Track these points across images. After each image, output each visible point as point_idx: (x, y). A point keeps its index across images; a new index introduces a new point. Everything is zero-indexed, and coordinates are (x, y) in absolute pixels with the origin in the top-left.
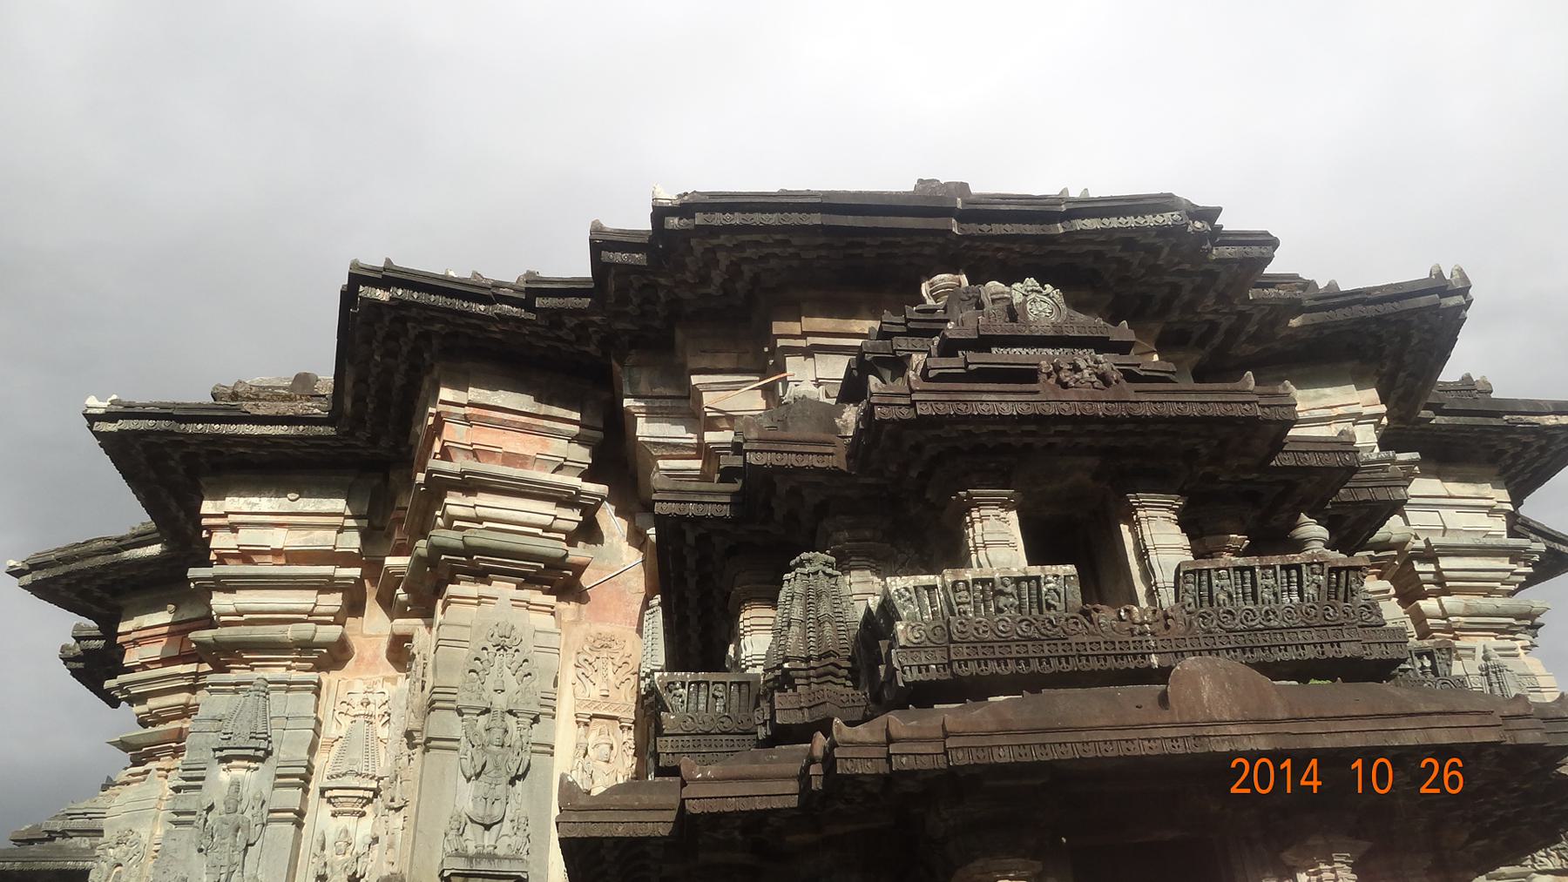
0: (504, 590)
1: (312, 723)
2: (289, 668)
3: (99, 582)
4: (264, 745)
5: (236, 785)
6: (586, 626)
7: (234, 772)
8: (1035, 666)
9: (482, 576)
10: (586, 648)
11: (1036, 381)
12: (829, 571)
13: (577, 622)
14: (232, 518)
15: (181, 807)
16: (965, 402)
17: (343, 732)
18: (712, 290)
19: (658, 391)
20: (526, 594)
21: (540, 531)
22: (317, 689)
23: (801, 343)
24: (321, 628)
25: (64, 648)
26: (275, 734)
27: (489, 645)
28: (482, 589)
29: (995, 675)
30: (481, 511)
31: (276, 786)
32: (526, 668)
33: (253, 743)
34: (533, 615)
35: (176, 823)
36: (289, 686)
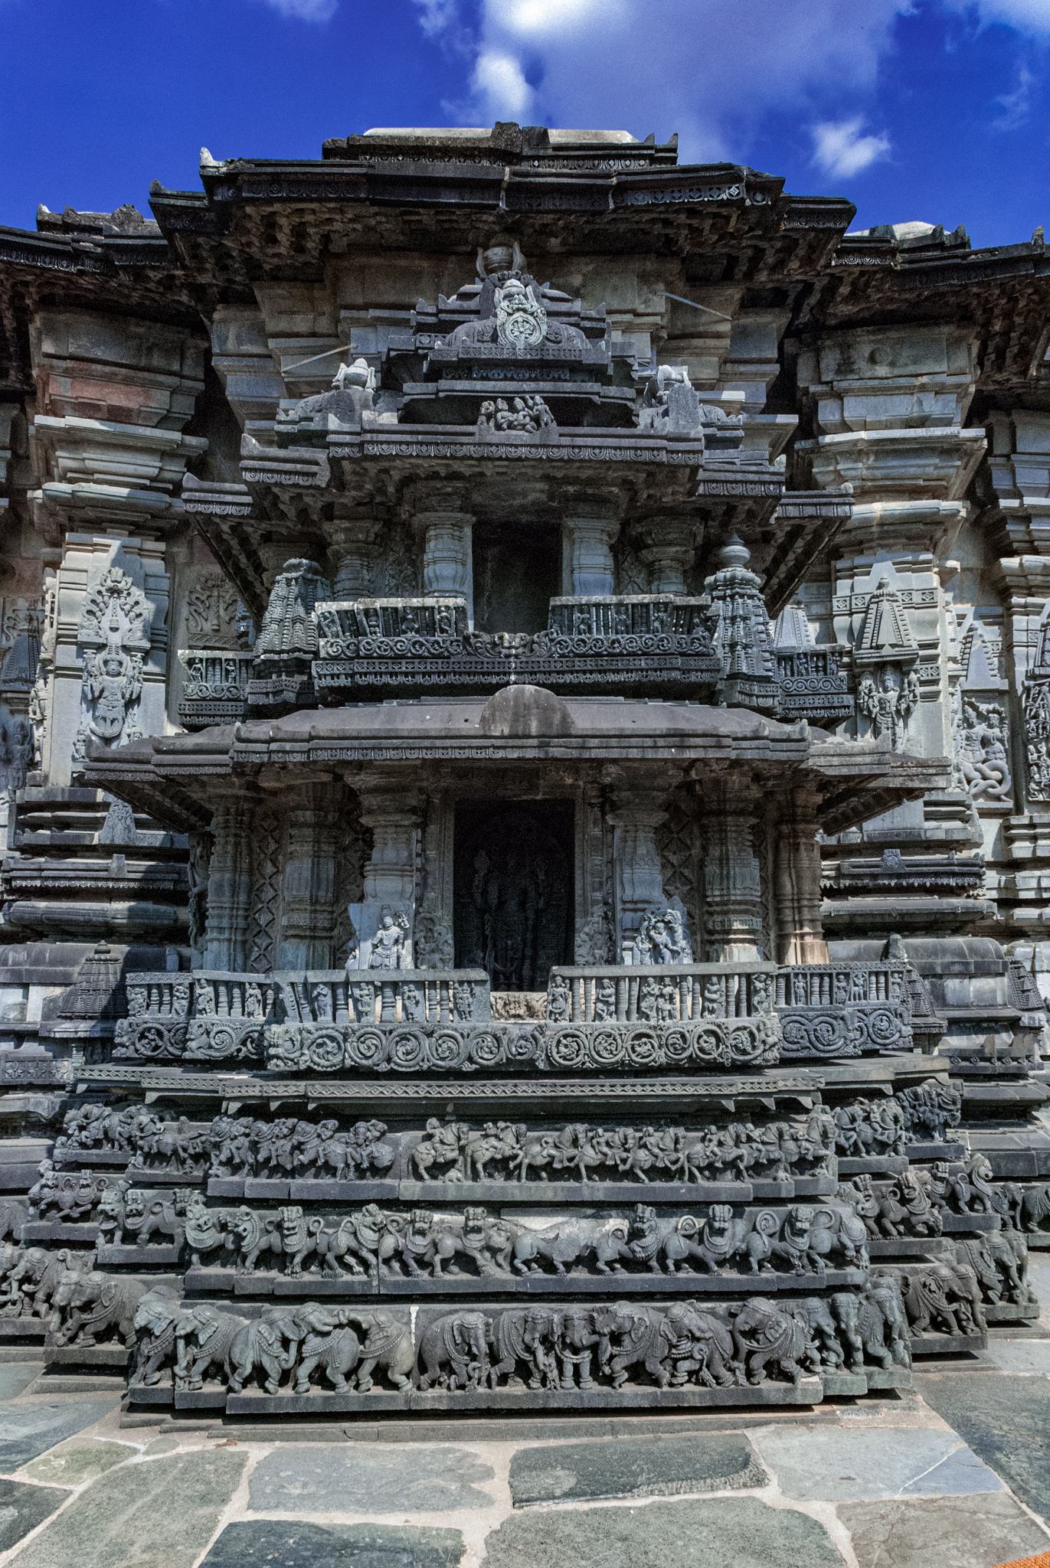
6: (198, 567)
8: (419, 679)
10: (198, 588)
11: (474, 423)
12: (310, 576)
18: (283, 250)
19: (247, 348)
20: (136, 541)
21: (147, 482)
23: (362, 314)
30: (90, 464)
32: (137, 610)
34: (145, 561)
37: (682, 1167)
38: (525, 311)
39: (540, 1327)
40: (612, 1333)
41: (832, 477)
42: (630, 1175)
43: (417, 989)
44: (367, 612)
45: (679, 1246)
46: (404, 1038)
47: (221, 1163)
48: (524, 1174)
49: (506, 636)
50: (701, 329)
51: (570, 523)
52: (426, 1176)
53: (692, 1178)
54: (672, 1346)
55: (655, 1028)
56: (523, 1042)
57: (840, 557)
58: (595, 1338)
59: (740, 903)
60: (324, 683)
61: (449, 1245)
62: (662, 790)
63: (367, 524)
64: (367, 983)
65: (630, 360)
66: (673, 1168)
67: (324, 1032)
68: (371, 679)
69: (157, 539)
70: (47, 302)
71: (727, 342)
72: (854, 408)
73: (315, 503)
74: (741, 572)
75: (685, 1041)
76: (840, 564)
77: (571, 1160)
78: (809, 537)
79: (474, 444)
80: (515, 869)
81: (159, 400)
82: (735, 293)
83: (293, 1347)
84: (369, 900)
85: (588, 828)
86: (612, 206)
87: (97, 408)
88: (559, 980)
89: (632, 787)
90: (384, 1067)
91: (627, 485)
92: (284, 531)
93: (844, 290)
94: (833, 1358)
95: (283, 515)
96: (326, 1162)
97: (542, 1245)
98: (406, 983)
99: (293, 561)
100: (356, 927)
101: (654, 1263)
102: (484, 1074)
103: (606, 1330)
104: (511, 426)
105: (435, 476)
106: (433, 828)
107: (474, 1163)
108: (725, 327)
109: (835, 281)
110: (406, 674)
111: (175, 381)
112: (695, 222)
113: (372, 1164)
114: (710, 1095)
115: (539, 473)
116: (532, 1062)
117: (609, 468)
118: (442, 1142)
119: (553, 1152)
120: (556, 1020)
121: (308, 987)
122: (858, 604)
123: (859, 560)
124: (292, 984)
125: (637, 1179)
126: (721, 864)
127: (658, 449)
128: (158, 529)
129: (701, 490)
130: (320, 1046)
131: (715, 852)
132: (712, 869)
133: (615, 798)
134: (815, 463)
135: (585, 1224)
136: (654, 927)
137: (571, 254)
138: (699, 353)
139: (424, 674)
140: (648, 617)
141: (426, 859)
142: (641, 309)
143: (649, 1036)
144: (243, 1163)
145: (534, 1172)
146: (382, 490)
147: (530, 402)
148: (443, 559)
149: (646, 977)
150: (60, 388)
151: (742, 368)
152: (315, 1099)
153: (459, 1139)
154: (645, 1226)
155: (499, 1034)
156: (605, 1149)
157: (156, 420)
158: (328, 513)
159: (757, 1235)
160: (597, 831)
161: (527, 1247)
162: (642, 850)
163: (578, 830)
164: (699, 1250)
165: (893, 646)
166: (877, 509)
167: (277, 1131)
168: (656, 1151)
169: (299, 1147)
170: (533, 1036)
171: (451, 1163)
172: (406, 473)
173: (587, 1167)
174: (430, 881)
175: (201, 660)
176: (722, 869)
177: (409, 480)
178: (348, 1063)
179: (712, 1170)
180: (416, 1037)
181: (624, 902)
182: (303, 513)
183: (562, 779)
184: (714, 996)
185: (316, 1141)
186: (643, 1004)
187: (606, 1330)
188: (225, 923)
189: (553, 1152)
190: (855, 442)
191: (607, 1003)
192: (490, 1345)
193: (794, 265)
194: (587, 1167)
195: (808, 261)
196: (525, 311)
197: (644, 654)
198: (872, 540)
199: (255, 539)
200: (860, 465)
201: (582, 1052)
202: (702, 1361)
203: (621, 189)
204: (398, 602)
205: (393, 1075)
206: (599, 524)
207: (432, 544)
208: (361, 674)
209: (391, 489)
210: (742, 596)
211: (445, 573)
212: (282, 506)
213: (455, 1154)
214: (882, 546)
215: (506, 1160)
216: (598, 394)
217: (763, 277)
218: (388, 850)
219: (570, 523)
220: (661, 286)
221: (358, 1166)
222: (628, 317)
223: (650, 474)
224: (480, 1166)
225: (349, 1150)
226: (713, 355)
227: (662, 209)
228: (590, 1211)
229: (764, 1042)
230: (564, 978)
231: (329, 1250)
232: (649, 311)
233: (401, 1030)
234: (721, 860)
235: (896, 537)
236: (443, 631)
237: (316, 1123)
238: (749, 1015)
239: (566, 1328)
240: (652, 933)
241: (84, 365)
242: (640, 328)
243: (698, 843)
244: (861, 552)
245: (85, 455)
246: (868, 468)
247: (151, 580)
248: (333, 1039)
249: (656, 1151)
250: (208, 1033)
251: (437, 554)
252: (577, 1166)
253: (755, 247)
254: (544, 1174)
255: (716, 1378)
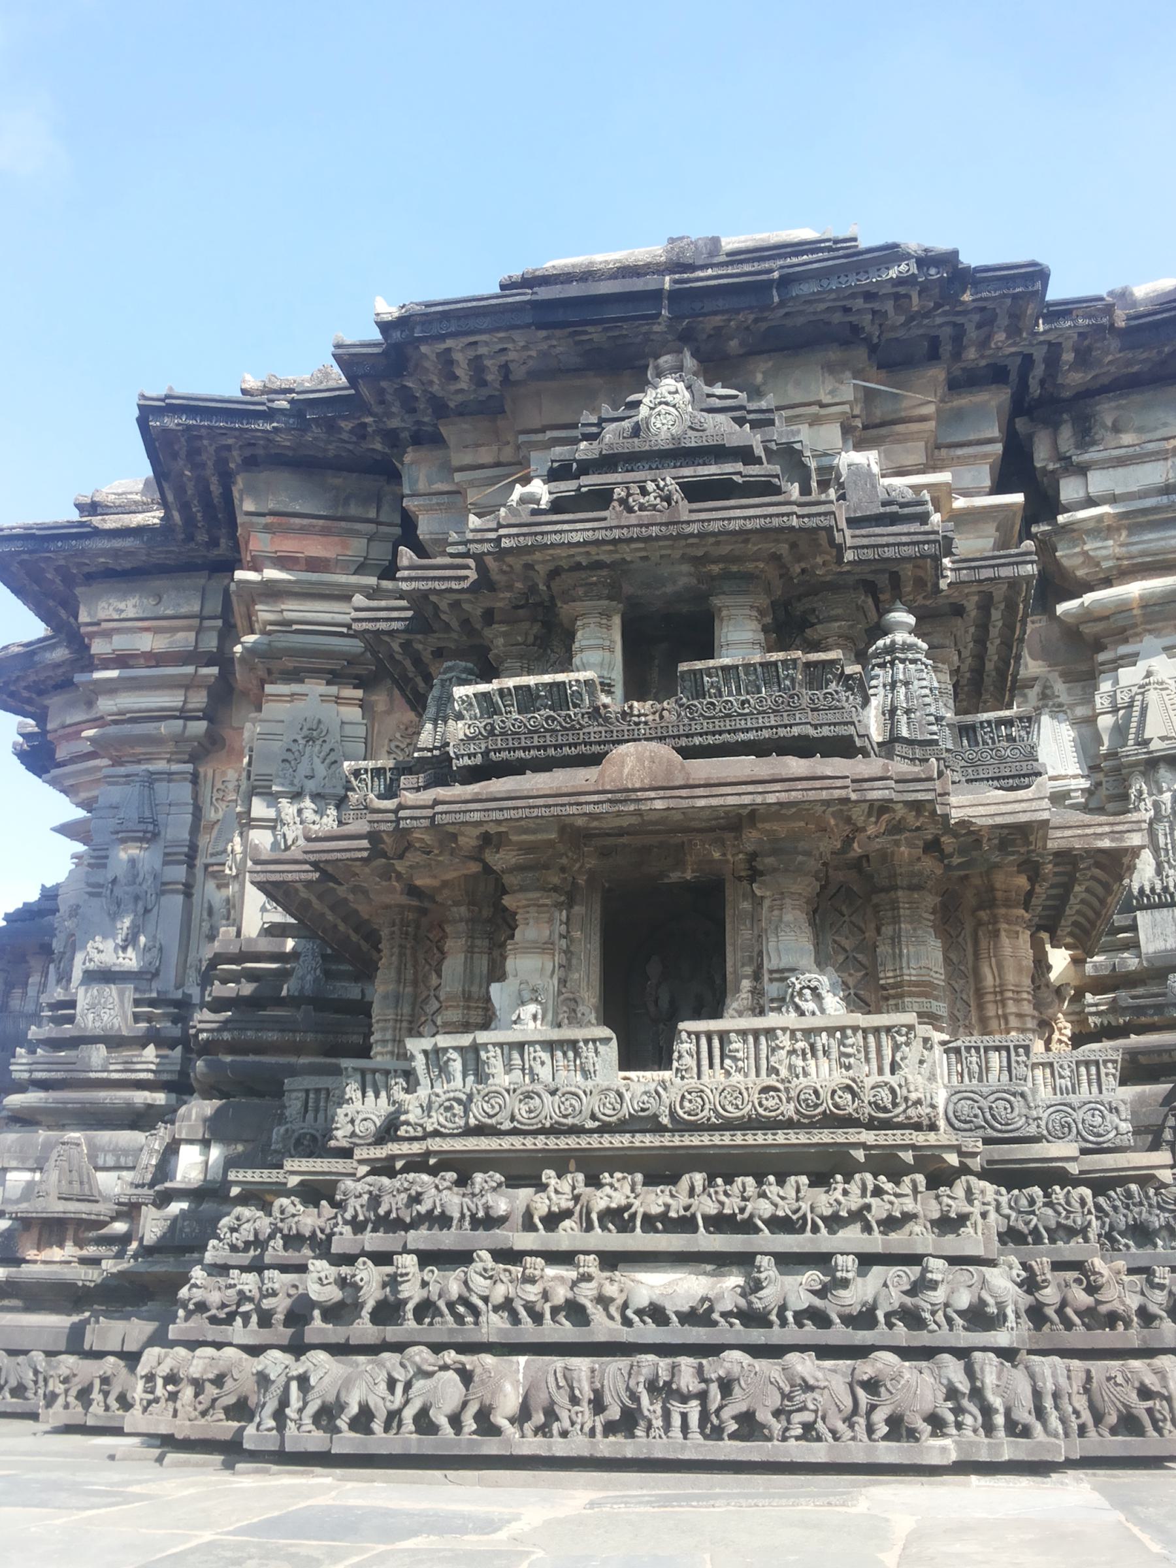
0: (316, 688)
1: (190, 809)
2: (169, 761)
3: (23, 684)
4: (151, 827)
5: (133, 862)
6: (397, 715)
7: (130, 851)
8: (551, 752)
9: (294, 676)
13: (389, 712)
14: (105, 625)
15: (92, 880)
16: (542, 533)
17: (220, 815)
20: (333, 690)
22: (195, 779)
24: (190, 724)
25: (15, 744)
26: (161, 818)
27: (299, 737)
28: (295, 688)
29: (520, 760)
31: (165, 863)
33: (142, 827)
34: (342, 709)
35: (91, 894)
36: (170, 776)
37: (804, 1217)
38: (667, 404)
39: (644, 1371)
40: (720, 1380)
41: (1080, 560)
42: (748, 1227)
43: (543, 1050)
44: (501, 692)
45: (802, 1300)
46: (528, 1096)
47: (346, 1222)
48: (638, 1223)
49: (636, 704)
50: (903, 414)
51: (717, 601)
52: (540, 1226)
53: (815, 1229)
54: (784, 1396)
55: (783, 1081)
56: (645, 1098)
57: (1101, 648)
58: (703, 1386)
59: (917, 984)
60: (461, 763)
61: (561, 1294)
62: (807, 853)
63: (525, 626)
64: (494, 1045)
65: (797, 446)
66: (794, 1217)
67: (452, 1095)
68: (504, 755)
69: (356, 687)
70: (251, 463)
71: (932, 425)
72: (1098, 482)
73: (475, 610)
74: (900, 637)
75: (818, 1097)
76: (1102, 657)
77: (686, 1209)
78: (1002, 606)
79: (606, 528)
80: (663, 949)
81: (357, 547)
82: (938, 373)
83: (399, 1388)
84: (511, 979)
85: (737, 905)
86: (776, 299)
87: (295, 560)
88: (684, 1036)
89: (774, 852)
90: (507, 1125)
91: (776, 558)
92: (452, 646)
93: (1068, 357)
94: (968, 1420)
95: (447, 627)
96: (443, 1212)
97: (655, 1299)
98: (532, 1043)
99: (449, 664)
100: (497, 1006)
101: (773, 1317)
102: (605, 1128)
103: (714, 1376)
104: (642, 508)
105: (578, 567)
106: (578, 910)
107: (588, 1213)
108: (930, 409)
109: (1054, 349)
110: (539, 748)
111: (371, 527)
112: (876, 306)
113: (487, 1214)
114: (835, 1144)
115: (677, 554)
116: (656, 1116)
117: (746, 541)
118: (557, 1192)
119: (670, 1201)
120: (683, 1078)
121: (438, 1051)
122: (1123, 698)
123: (1123, 650)
124: (425, 1052)
125: (757, 1230)
126: (893, 944)
127: (788, 515)
128: (357, 677)
129: (849, 556)
130: (448, 1109)
131: (887, 930)
132: (884, 949)
133: (760, 867)
134: (1059, 546)
135: (703, 1280)
136: (800, 994)
137: (752, 352)
138: (903, 439)
139: (556, 747)
140: (778, 676)
141: (572, 941)
142: (827, 400)
143: (776, 1090)
144: (367, 1221)
145: (649, 1223)
146: (533, 589)
147: (662, 484)
148: (590, 647)
149: (774, 1029)
150: (259, 543)
151: (960, 452)
152: (436, 1153)
153: (574, 1188)
154: (762, 1276)
155: (623, 1090)
156: (723, 1198)
157: (353, 568)
158: (489, 617)
159: (881, 1288)
160: (746, 905)
161: (642, 1299)
162: (788, 917)
163: (728, 907)
164: (818, 1302)
165: (1162, 739)
166: (1134, 589)
167: (398, 1184)
168: (778, 1200)
169: (417, 1199)
170: (657, 1092)
171: (567, 1214)
172: (551, 566)
173: (704, 1217)
174: (574, 961)
175: (366, 771)
176: (893, 948)
177: (555, 573)
178: (472, 1122)
179: (834, 1222)
180: (539, 1096)
181: (771, 972)
182: (466, 623)
183: (710, 853)
184: (849, 1050)
185: (433, 1191)
186: (772, 1059)
187: (714, 1376)
188: (388, 1036)
189: (670, 1201)
190: (1100, 518)
191: (735, 1059)
192: (596, 1391)
193: (1001, 336)
194: (706, 1218)
195: (1014, 331)
196: (667, 404)
197: (774, 711)
198: (1135, 626)
199: (427, 656)
200: (1111, 542)
201: (707, 1106)
202: (816, 1411)
203: (786, 281)
204: (531, 680)
205: (514, 1132)
206: (741, 600)
207: (579, 635)
208: (495, 751)
209: (542, 587)
210: (903, 661)
211: (592, 660)
212: (443, 617)
213: (571, 1204)
214: (1150, 631)
215: (621, 1210)
216: (740, 473)
217: (971, 354)
218: (529, 931)
219: (717, 601)
220: (848, 374)
221: (473, 1216)
222: (815, 409)
223: (793, 546)
224: (594, 1216)
225: (466, 1199)
226: (918, 440)
227: (833, 296)
228: (709, 1268)
229: (906, 1099)
230: (689, 1034)
231: (440, 1296)
232: (837, 400)
233: (524, 1089)
234: (892, 939)
235: (1165, 620)
236: (575, 706)
237: (435, 1176)
238: (893, 1073)
239: (673, 1375)
240: (797, 1000)
241: (284, 519)
242: (828, 419)
243: (873, 926)
244: (1126, 641)
245: (283, 607)
246: (1121, 545)
247: (347, 727)
248: (459, 1101)
249: (778, 1200)
250: (352, 1122)
251: (584, 643)
252: (694, 1216)
253: (955, 325)
254: (660, 1226)
255: (834, 1433)
